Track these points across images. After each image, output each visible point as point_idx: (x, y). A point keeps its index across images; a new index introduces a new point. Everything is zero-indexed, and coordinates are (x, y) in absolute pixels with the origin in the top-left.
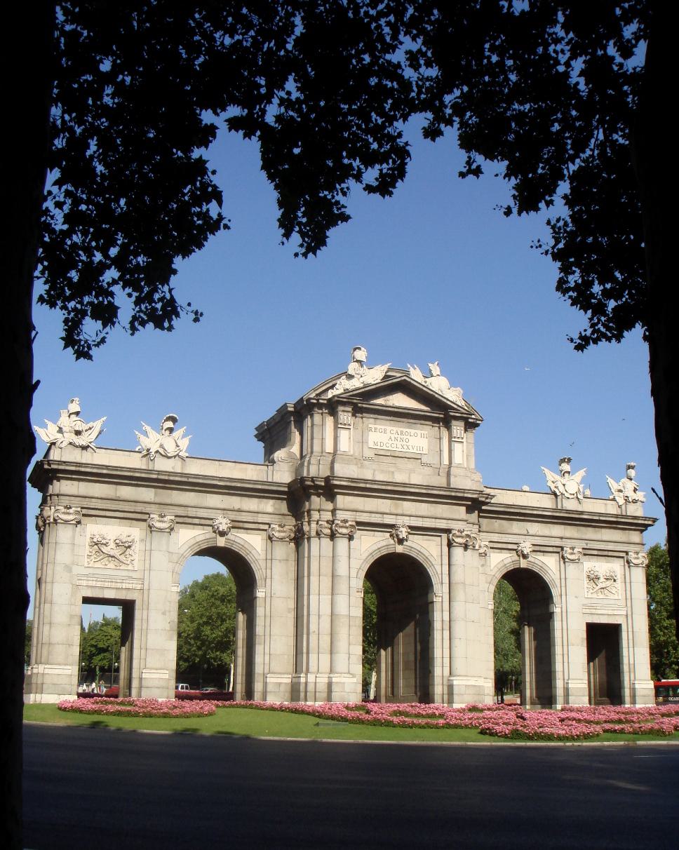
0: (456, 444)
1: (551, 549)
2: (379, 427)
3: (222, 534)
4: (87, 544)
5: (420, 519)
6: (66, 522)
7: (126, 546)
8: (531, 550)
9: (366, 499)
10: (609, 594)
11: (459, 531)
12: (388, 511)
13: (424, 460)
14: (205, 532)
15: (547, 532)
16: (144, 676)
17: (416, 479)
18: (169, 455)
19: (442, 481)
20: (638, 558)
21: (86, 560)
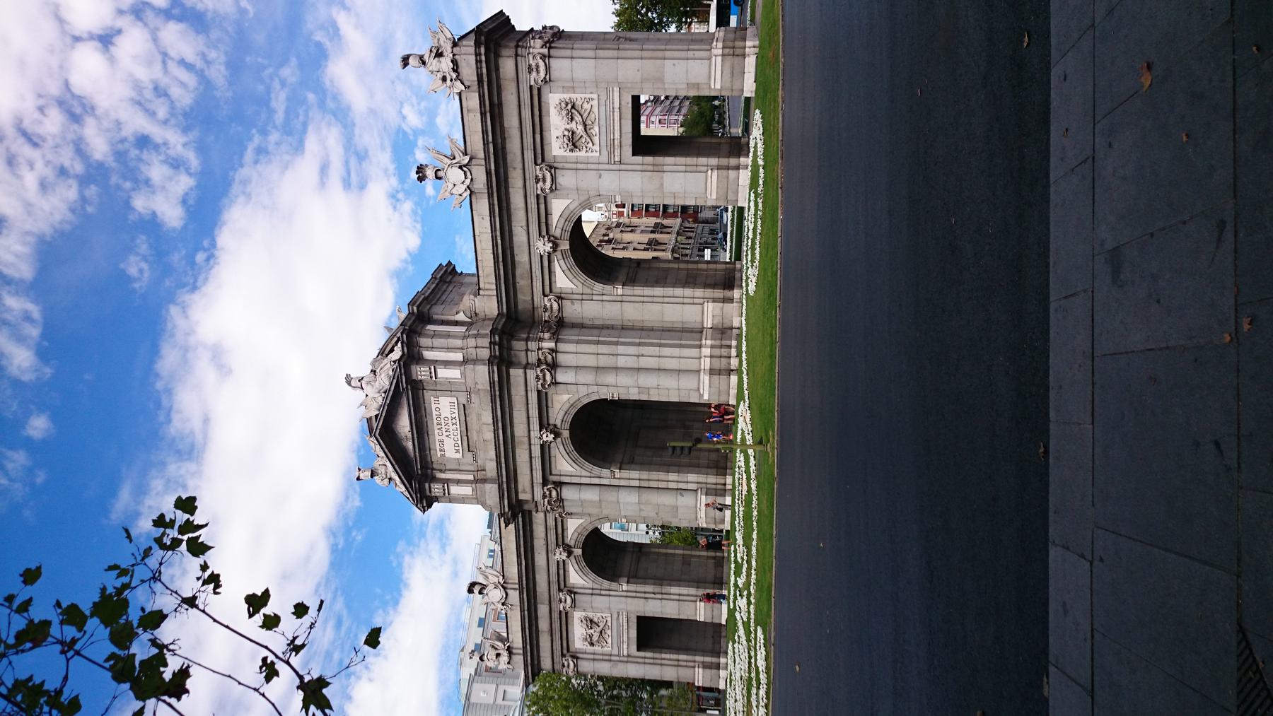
0: (439, 376)
1: (542, 207)
2: (438, 448)
3: (570, 553)
4: (591, 648)
5: (531, 419)
6: (576, 666)
7: (591, 623)
8: (546, 239)
9: (519, 472)
10: (592, 116)
11: (537, 382)
12: (527, 452)
13: (463, 400)
14: (570, 564)
15: (521, 214)
16: (702, 620)
17: (488, 418)
18: (505, 596)
19: (487, 399)
20: (537, 67)
21: (605, 649)
